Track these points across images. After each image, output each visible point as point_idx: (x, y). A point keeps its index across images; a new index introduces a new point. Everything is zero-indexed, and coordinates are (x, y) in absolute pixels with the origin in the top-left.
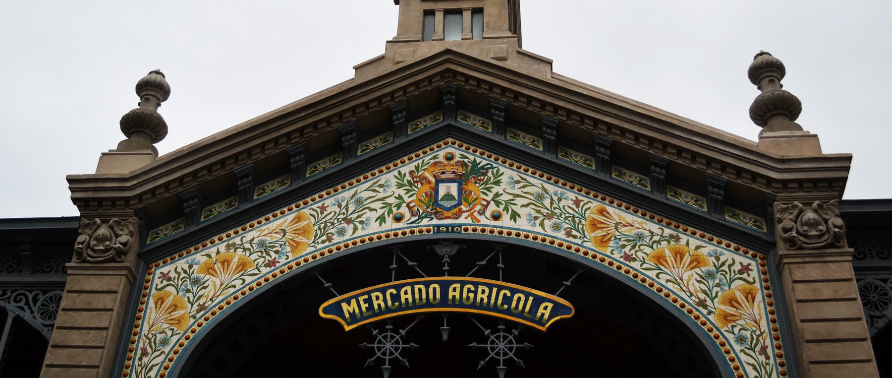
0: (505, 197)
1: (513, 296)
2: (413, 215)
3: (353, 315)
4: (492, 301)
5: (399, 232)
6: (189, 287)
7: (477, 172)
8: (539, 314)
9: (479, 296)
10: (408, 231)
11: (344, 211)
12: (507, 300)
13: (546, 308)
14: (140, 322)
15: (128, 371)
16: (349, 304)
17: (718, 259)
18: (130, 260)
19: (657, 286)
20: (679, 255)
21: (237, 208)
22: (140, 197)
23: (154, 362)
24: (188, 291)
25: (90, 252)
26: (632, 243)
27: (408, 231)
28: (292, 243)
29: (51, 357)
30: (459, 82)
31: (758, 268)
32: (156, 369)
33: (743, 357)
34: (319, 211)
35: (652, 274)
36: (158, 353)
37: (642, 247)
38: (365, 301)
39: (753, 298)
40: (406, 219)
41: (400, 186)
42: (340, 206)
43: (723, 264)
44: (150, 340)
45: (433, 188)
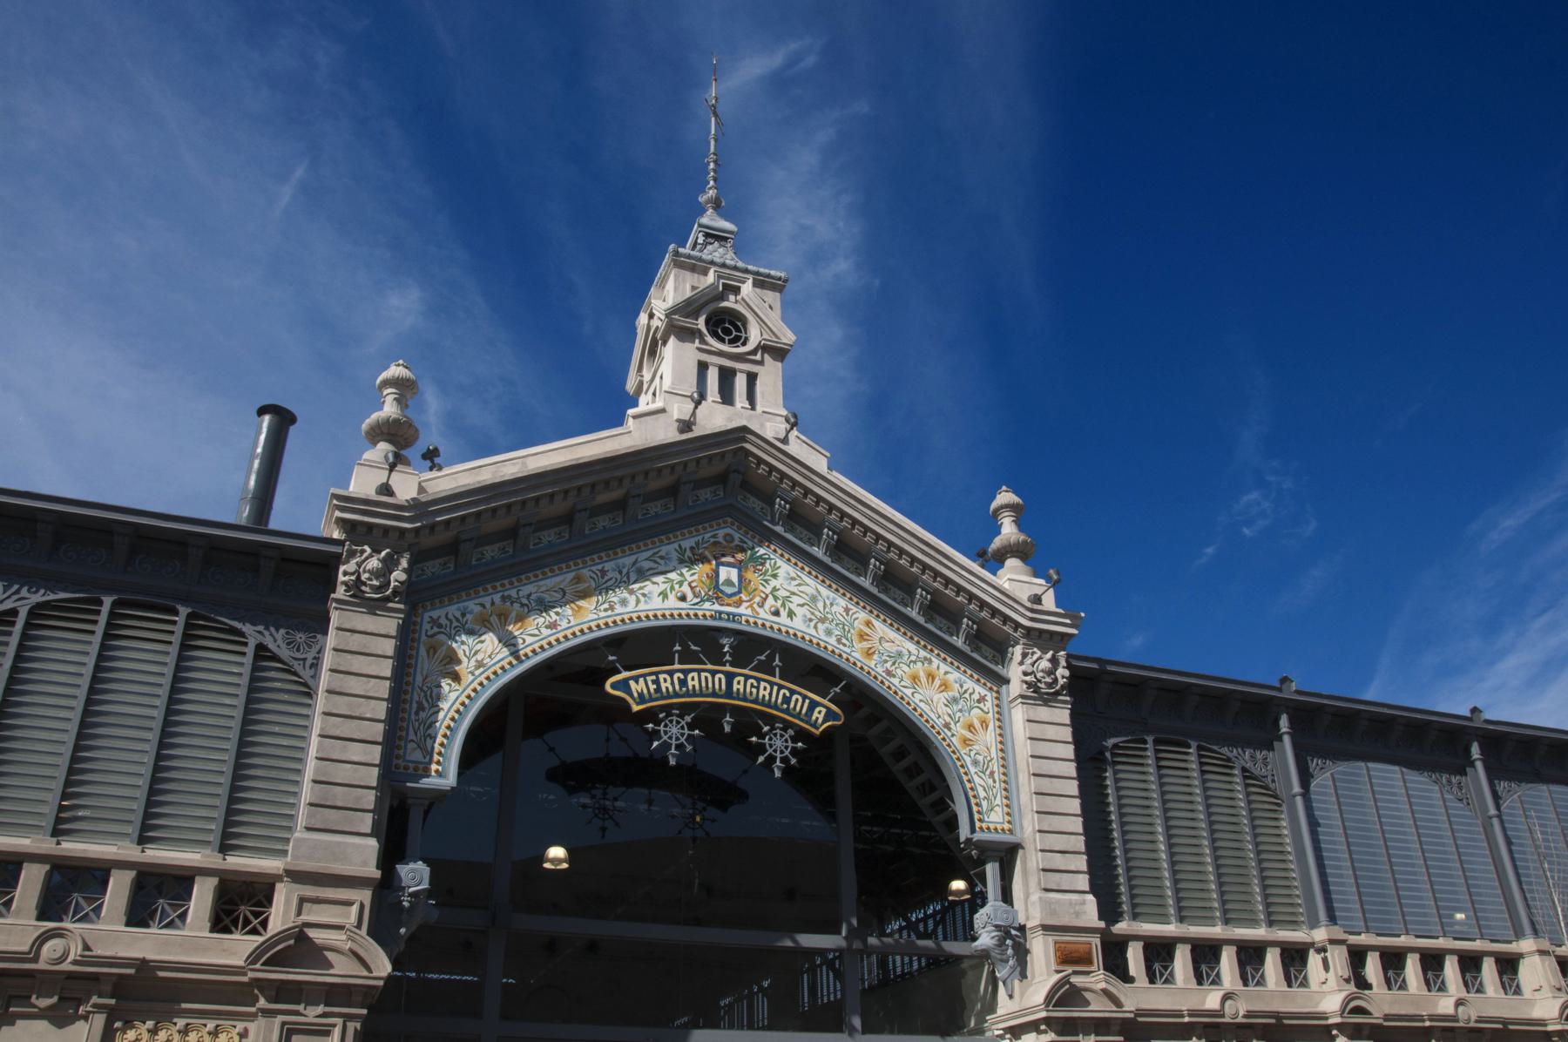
0: (782, 593)
3: (641, 695)
9: (762, 692)
12: (787, 700)
20: (931, 676)
35: (909, 692)
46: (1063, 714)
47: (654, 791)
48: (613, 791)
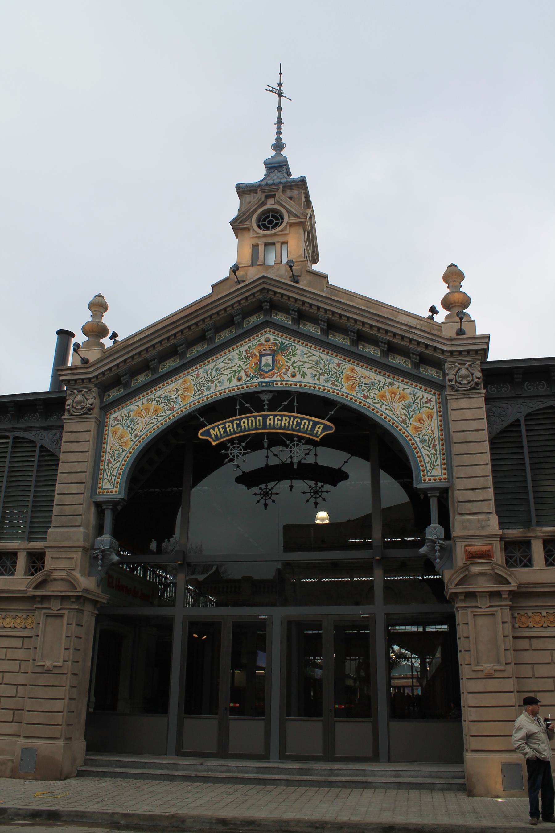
1: (301, 421)
2: (248, 377)
3: (216, 436)
4: (291, 425)
5: (240, 387)
6: (129, 424)
7: (283, 348)
8: (315, 431)
9: (284, 422)
10: (245, 386)
11: (209, 376)
12: (299, 424)
13: (319, 428)
14: (105, 445)
15: (102, 472)
16: (214, 430)
17: (414, 396)
18: (96, 412)
19: (380, 412)
20: (393, 394)
21: (150, 378)
22: (97, 377)
23: (115, 467)
24: (129, 427)
25: (74, 410)
26: (368, 388)
27: (245, 386)
28: (182, 396)
29: (62, 468)
30: (271, 294)
31: (436, 400)
32: (116, 470)
33: (423, 450)
34: (195, 376)
35: (378, 406)
36: (116, 461)
37: (373, 390)
38: (223, 428)
39: (432, 418)
40: (244, 379)
41: (240, 359)
42: (207, 373)
43: (417, 399)
44: (111, 455)
45: (258, 360)
46: (481, 402)
47: (294, 481)
48: (270, 485)
